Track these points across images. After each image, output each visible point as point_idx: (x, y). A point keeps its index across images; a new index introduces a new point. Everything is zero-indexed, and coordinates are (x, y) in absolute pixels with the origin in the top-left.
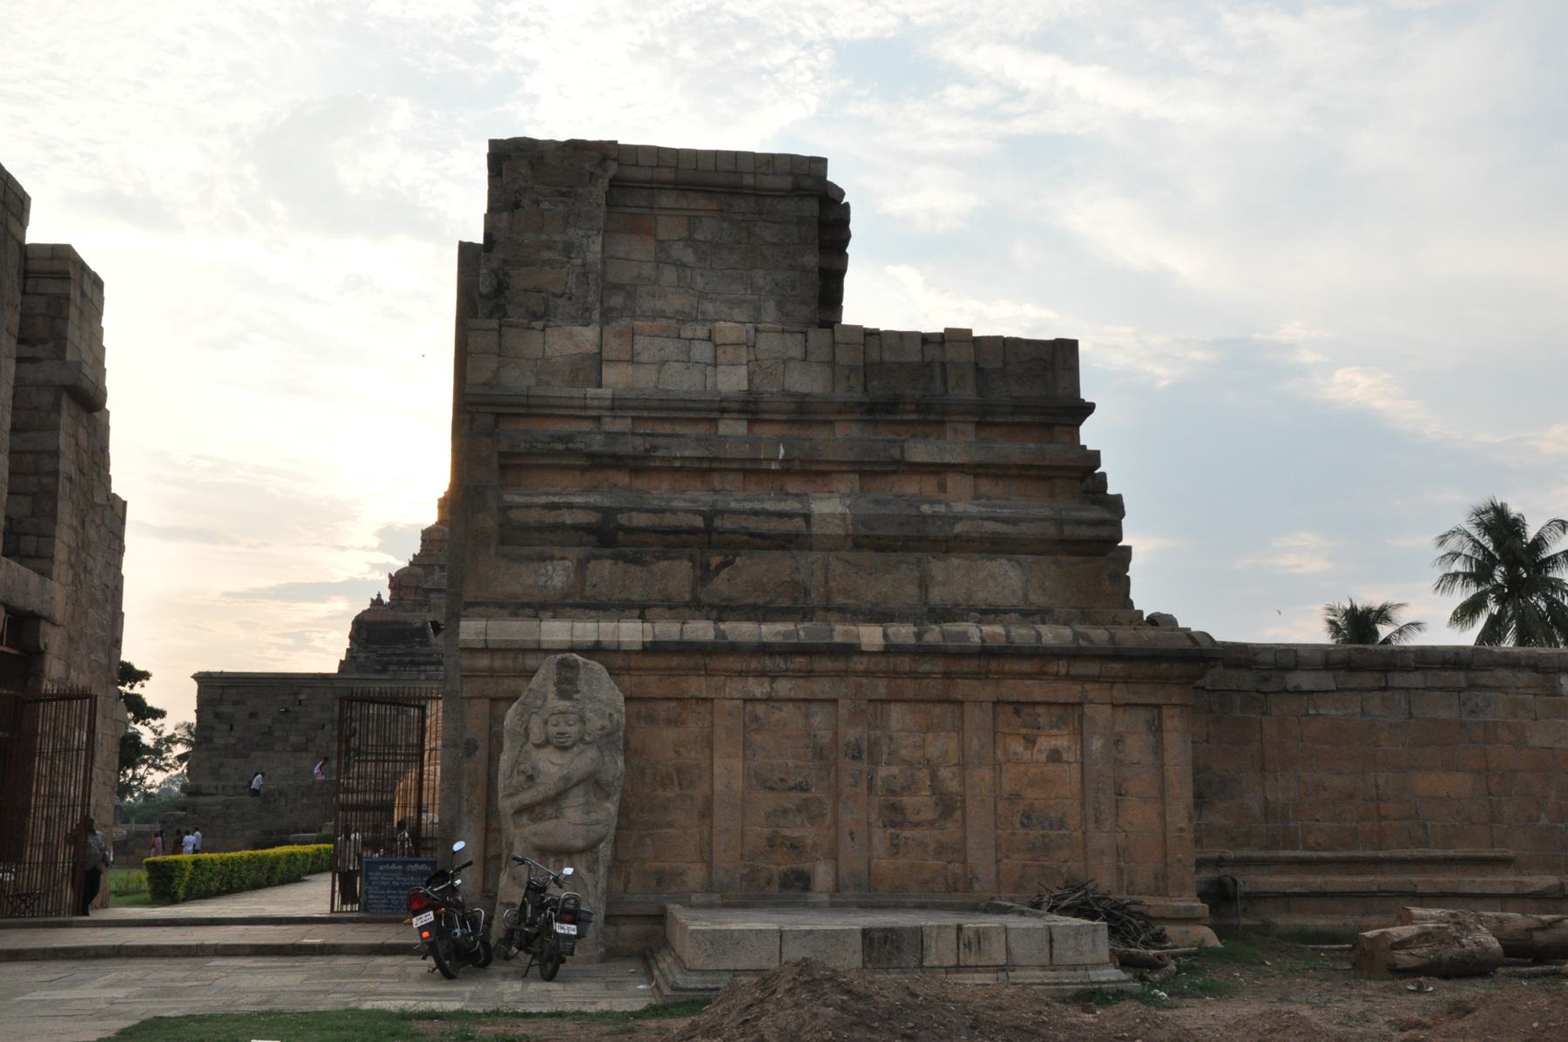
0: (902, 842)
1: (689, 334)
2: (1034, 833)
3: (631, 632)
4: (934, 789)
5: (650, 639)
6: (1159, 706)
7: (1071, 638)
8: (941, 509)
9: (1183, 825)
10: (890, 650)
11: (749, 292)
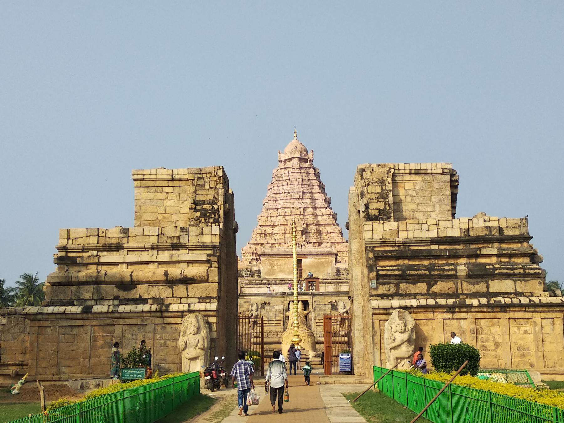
0: (486, 355)
1: (421, 223)
2: (521, 352)
3: (414, 303)
5: (419, 304)
6: (554, 318)
7: (529, 301)
8: (491, 267)
9: (561, 350)
10: (480, 305)
11: (431, 202)
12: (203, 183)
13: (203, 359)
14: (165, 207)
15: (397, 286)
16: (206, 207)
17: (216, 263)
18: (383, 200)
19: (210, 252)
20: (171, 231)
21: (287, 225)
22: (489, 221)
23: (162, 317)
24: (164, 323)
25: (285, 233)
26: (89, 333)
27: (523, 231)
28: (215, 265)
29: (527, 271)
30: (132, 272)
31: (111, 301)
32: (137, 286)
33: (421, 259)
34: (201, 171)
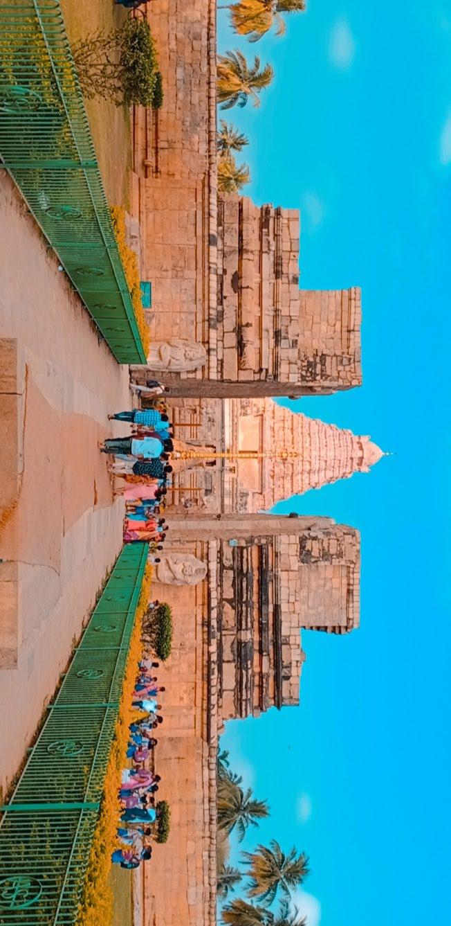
3: (213, 585)
4: (173, 665)
5: (212, 590)
6: (195, 727)
8: (249, 666)
10: (209, 654)
12: (344, 363)
14: (319, 323)
15: (231, 568)
16: (319, 367)
17: (258, 378)
18: (321, 555)
19: (270, 371)
20: (293, 330)
21: (293, 443)
22: (297, 666)
23: (204, 321)
24: (197, 323)
25: (284, 441)
26: (188, 243)
27: (286, 702)
28: (257, 377)
29: (244, 703)
30: (251, 289)
31: (222, 266)
32: (237, 294)
33: (259, 593)
34: (357, 362)
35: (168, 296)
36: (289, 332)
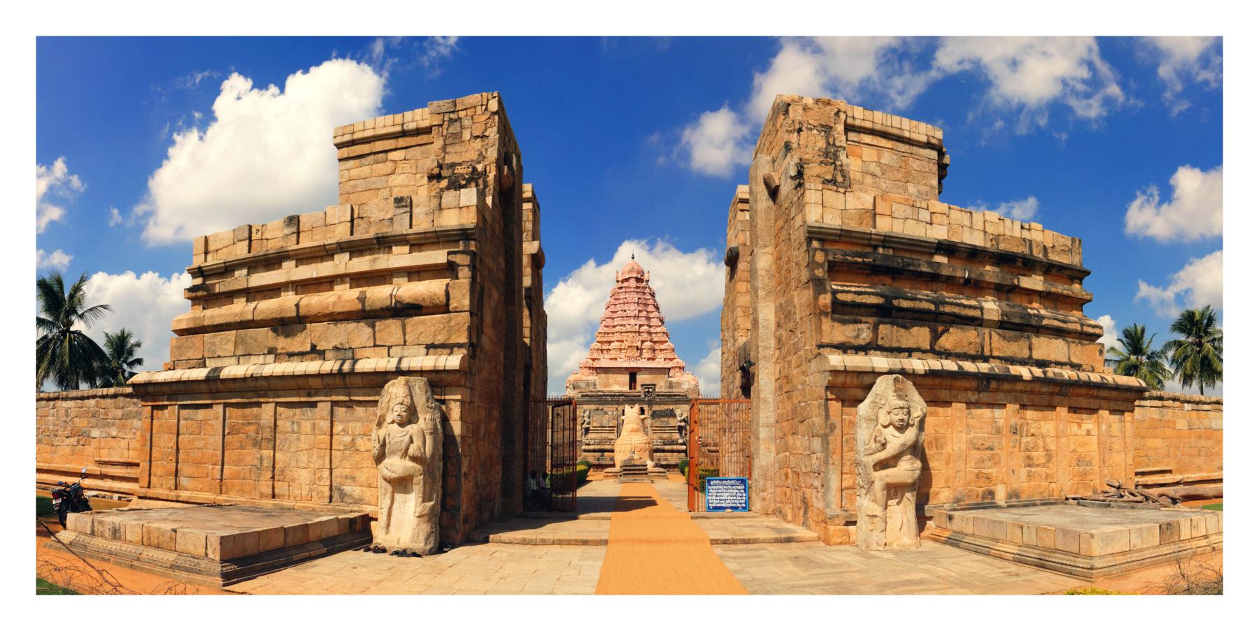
12: (458, 130)
13: (422, 483)
16: (459, 170)
34: (455, 106)
35: (303, 458)
36: (382, 215)
